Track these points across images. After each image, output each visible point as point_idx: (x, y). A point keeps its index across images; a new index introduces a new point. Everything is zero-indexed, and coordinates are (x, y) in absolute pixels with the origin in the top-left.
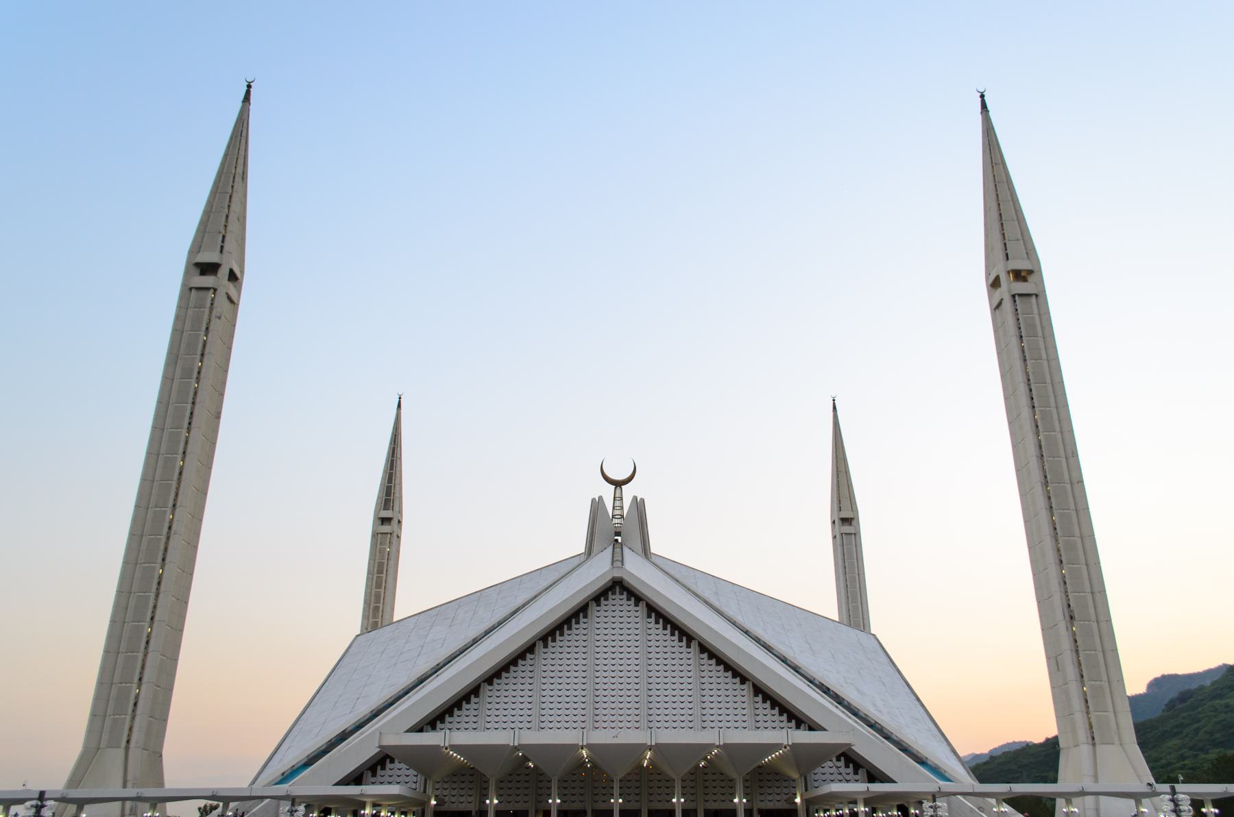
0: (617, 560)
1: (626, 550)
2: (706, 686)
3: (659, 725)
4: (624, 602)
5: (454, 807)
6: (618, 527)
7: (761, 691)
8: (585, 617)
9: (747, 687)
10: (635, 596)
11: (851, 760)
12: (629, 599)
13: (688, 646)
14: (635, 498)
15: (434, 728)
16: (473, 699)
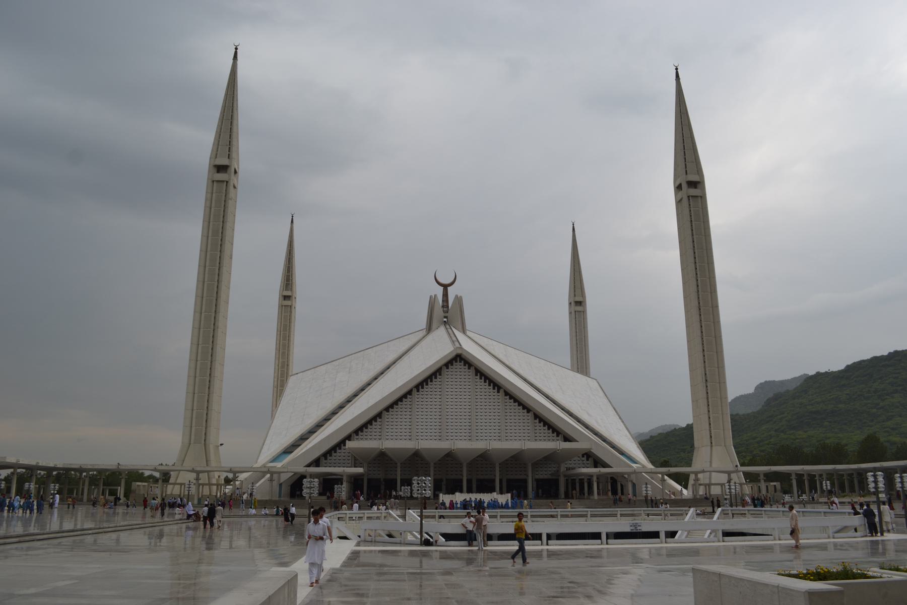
2: (508, 414)
4: (462, 367)
6: (446, 312)
7: (538, 417)
13: (498, 392)
14: (457, 296)
15: (357, 435)
16: (379, 420)
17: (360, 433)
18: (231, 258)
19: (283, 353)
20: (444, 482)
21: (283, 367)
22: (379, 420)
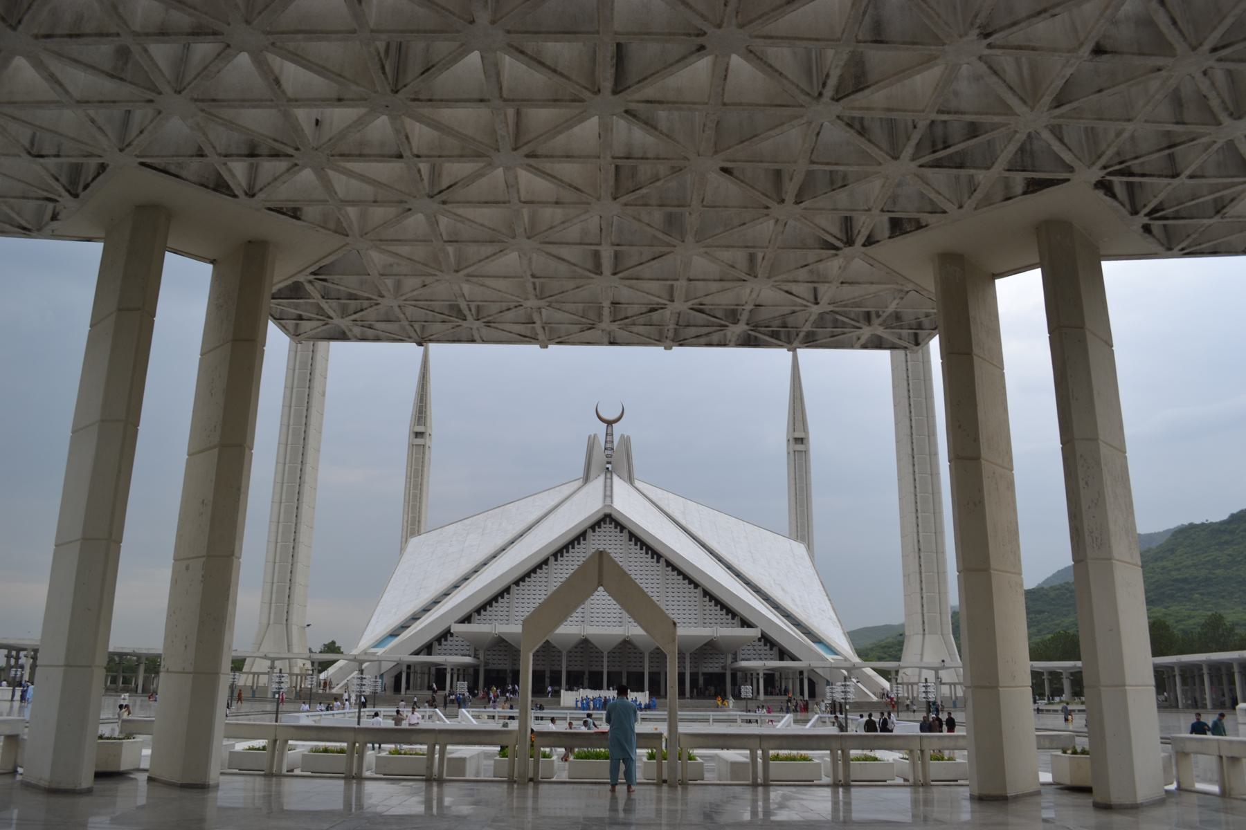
0: (608, 494)
1: (615, 478)
5: (495, 667)
9: (699, 590)
11: (765, 639)
14: (622, 436)
16: (506, 596)
17: (483, 613)
18: (324, 395)
19: (414, 506)
20: (587, 675)
21: (413, 524)
22: (506, 596)
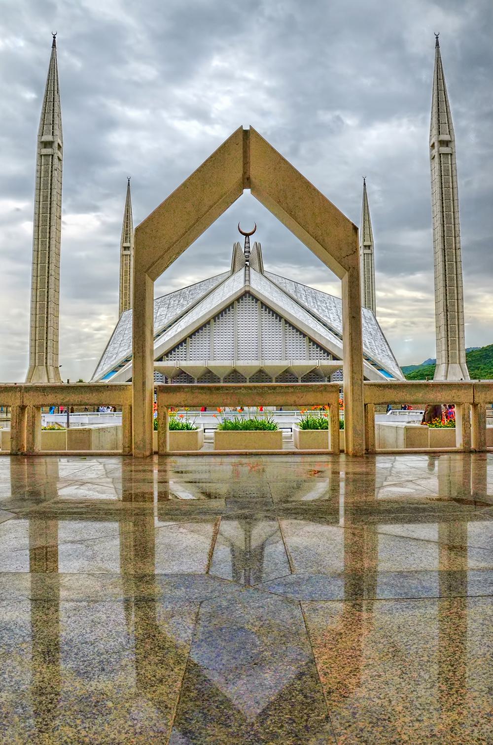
0: (247, 279)
3: (266, 358)
4: (251, 301)
8: (233, 308)
10: (256, 299)
12: (253, 300)
13: (280, 321)
16: (184, 345)
